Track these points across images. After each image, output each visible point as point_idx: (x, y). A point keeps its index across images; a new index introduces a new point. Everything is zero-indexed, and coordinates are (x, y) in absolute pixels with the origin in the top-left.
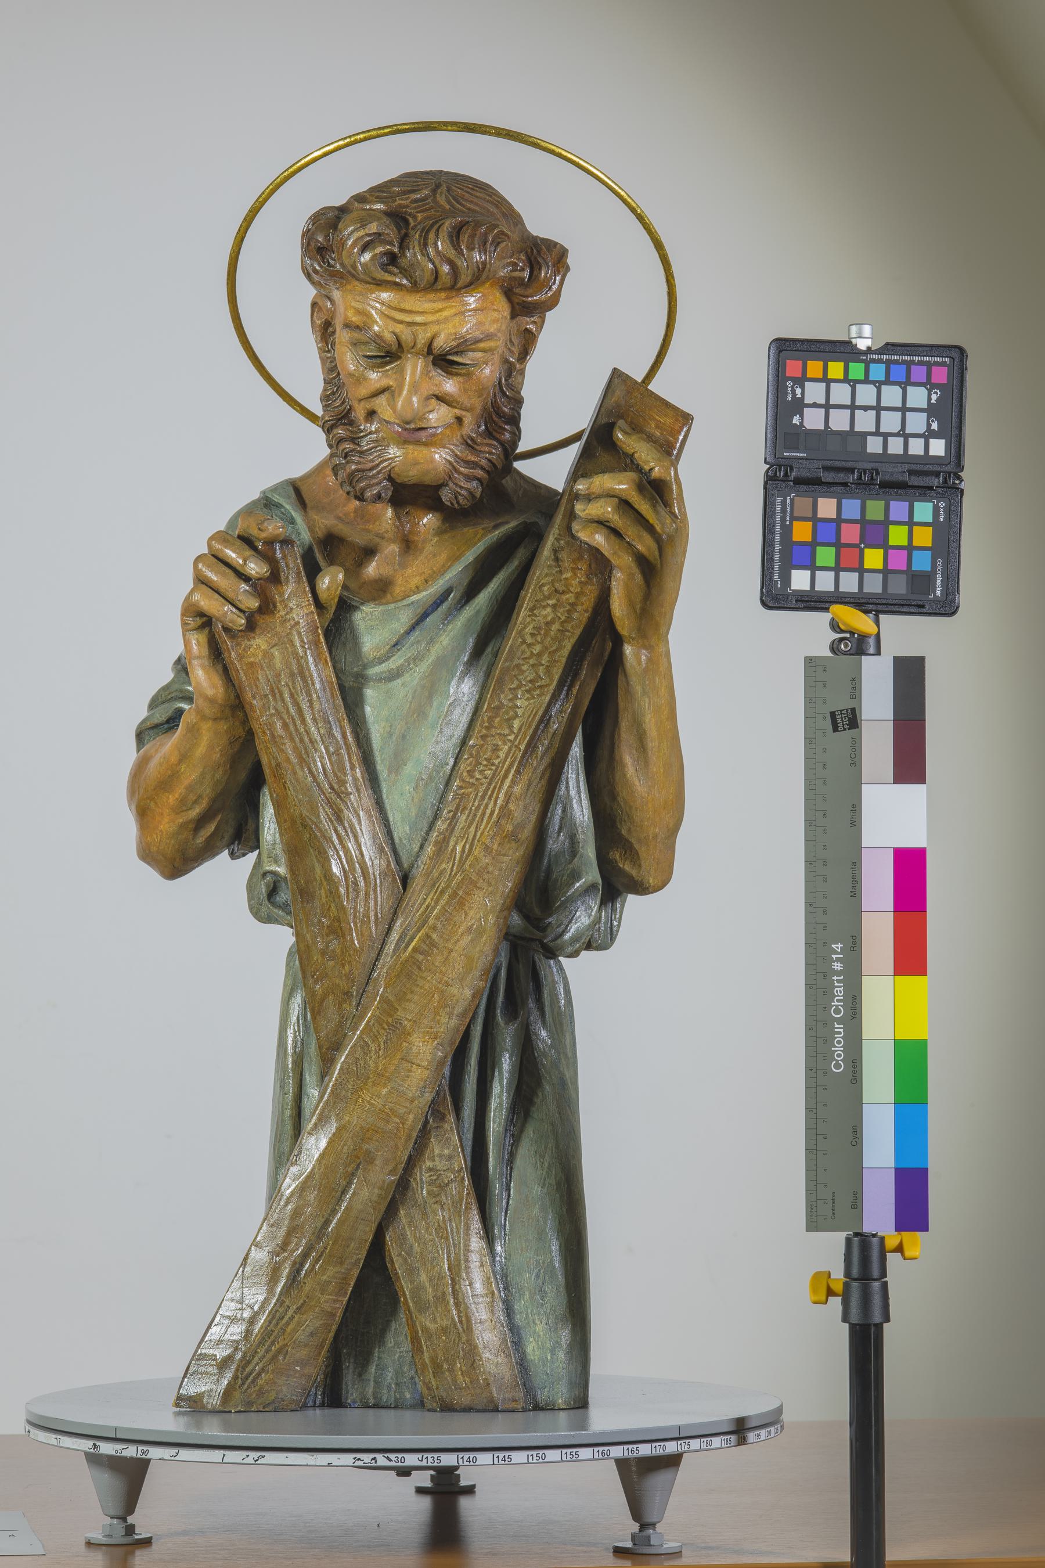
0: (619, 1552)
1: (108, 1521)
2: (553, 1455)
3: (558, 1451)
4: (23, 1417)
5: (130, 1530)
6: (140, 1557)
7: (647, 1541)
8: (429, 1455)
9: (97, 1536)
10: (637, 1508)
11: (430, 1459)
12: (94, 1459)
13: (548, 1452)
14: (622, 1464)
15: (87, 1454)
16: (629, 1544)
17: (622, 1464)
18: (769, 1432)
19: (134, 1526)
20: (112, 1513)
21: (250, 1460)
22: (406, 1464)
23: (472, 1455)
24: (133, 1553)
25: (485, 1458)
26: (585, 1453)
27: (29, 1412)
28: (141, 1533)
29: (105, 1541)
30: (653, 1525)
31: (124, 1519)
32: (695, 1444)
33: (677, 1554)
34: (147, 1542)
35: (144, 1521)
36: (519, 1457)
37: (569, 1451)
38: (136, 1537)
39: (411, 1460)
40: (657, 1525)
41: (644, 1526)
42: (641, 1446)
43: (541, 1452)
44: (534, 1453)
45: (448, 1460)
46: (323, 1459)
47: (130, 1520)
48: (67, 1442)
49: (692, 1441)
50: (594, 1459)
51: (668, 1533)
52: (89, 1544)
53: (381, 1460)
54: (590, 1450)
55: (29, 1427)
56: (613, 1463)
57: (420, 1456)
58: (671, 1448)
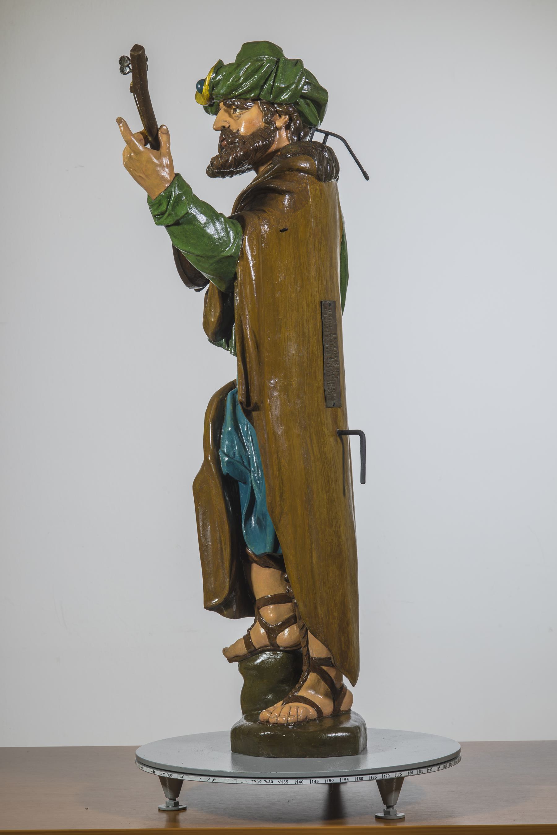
0: (377, 817)
5: (177, 804)
6: (182, 816)
9: (163, 806)
10: (385, 800)
16: (382, 814)
19: (178, 803)
24: (178, 814)
28: (182, 805)
30: (392, 806)
32: (404, 773)
33: (402, 819)
34: (184, 809)
35: (182, 800)
38: (180, 807)
40: (394, 806)
41: (388, 807)
52: (160, 810)
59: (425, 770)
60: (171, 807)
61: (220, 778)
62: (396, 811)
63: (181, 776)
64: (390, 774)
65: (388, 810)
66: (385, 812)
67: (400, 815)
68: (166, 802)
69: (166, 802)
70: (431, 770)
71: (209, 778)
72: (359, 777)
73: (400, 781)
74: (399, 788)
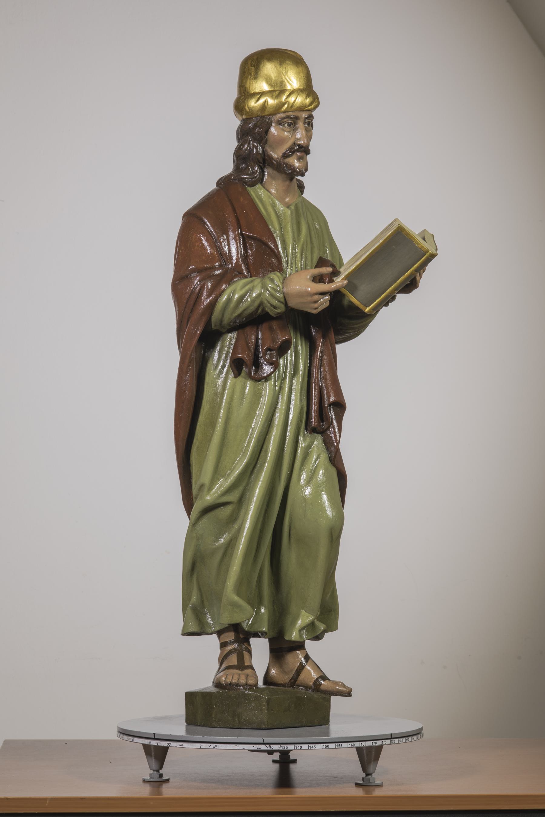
0: (357, 785)
1: (151, 772)
2: (332, 746)
3: (334, 744)
4: (117, 730)
5: (161, 776)
7: (369, 781)
8: (283, 746)
9: (147, 778)
10: (364, 768)
11: (283, 748)
12: (146, 747)
13: (330, 745)
14: (359, 750)
15: (144, 746)
16: (361, 782)
17: (359, 750)
18: (418, 737)
20: (154, 769)
21: (212, 747)
22: (274, 749)
23: (300, 745)
24: (162, 785)
25: (305, 747)
26: (345, 745)
27: (118, 728)
28: (165, 778)
29: (152, 780)
30: (371, 774)
31: (158, 771)
32: (388, 742)
34: (167, 781)
35: (166, 772)
36: (318, 746)
37: (338, 744)
39: (276, 747)
41: (367, 775)
42: (367, 742)
43: (327, 744)
44: (325, 745)
45: (290, 747)
46: (241, 747)
47: (161, 772)
48: (137, 740)
49: (387, 741)
50: (348, 747)
51: (377, 777)
52: (144, 781)
53: (263, 747)
54: (347, 744)
55: (119, 734)
56: (354, 750)
57: (279, 746)
58: (379, 743)
59: (404, 740)
60: (156, 778)
61: (221, 745)
62: (374, 779)
63: (181, 744)
64: (377, 741)
65: (368, 777)
66: (363, 779)
67: (378, 782)
68: (150, 774)
69: (150, 774)
70: (408, 740)
71: (210, 745)
72: (351, 743)
73: (379, 749)
74: (377, 758)
